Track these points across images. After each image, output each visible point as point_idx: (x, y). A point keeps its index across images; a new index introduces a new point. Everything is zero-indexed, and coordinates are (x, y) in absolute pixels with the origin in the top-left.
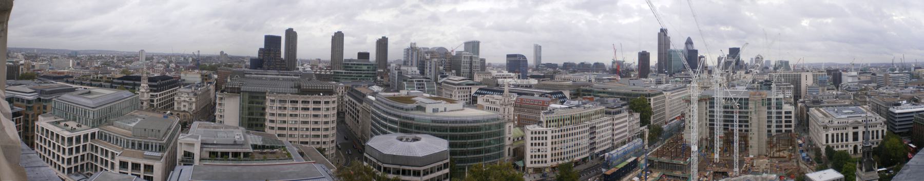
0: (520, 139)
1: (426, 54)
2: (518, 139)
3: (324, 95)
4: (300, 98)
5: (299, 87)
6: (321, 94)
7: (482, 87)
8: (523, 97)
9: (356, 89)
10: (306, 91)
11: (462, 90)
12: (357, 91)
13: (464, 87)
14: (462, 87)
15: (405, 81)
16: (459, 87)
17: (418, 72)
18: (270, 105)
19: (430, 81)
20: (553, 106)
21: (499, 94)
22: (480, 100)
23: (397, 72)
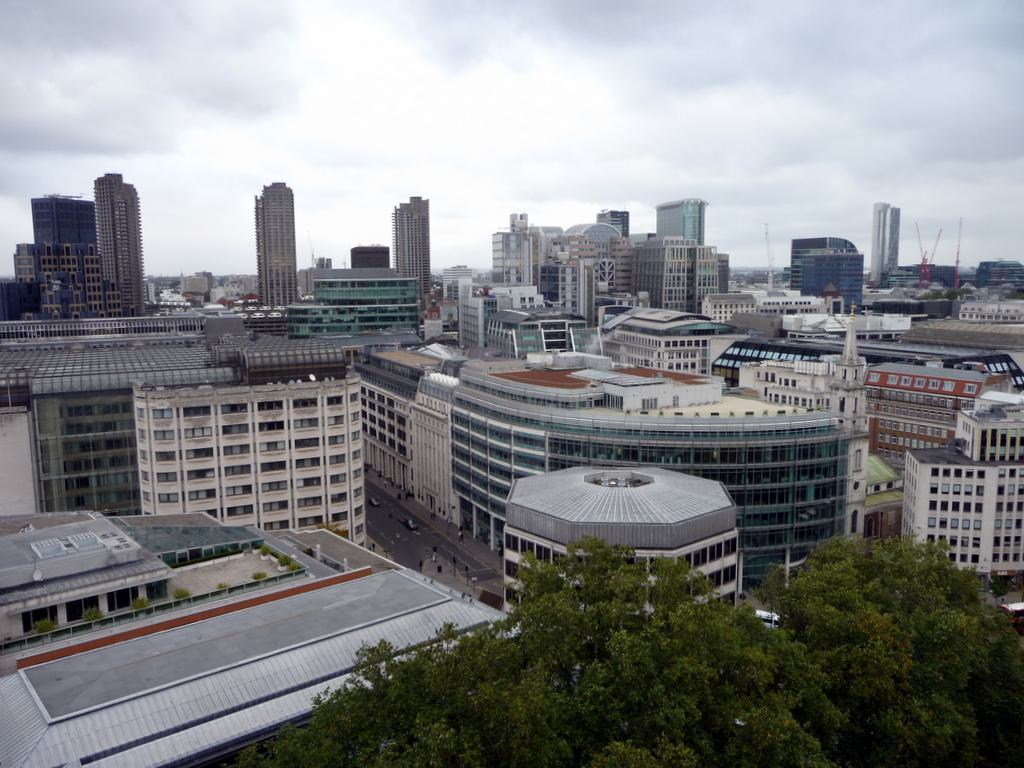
0: (883, 488)
1: (558, 248)
2: (877, 488)
3: (320, 379)
4: (253, 395)
5: (235, 362)
6: (312, 377)
7: (742, 338)
8: (886, 367)
9: (380, 355)
10: (264, 373)
11: (686, 347)
12: (378, 362)
13: (686, 339)
14: (679, 339)
15: (509, 326)
16: (671, 339)
17: (539, 300)
18: (153, 428)
19: (582, 325)
20: (993, 396)
21: (806, 358)
22: (747, 377)
23: (479, 302)
